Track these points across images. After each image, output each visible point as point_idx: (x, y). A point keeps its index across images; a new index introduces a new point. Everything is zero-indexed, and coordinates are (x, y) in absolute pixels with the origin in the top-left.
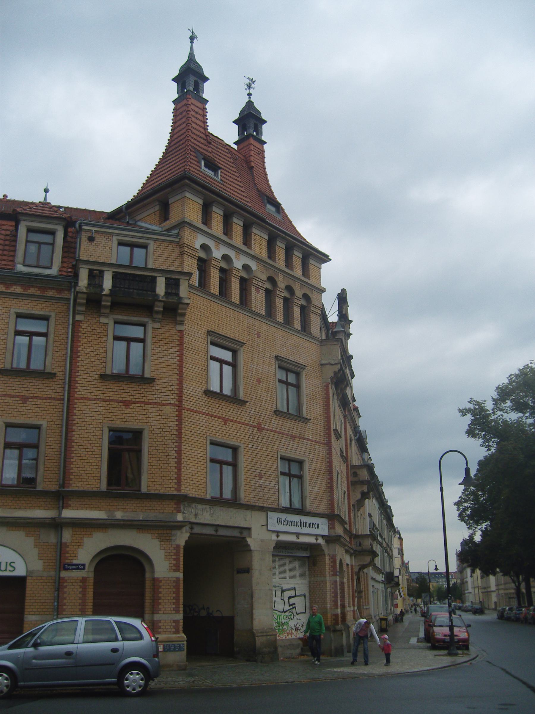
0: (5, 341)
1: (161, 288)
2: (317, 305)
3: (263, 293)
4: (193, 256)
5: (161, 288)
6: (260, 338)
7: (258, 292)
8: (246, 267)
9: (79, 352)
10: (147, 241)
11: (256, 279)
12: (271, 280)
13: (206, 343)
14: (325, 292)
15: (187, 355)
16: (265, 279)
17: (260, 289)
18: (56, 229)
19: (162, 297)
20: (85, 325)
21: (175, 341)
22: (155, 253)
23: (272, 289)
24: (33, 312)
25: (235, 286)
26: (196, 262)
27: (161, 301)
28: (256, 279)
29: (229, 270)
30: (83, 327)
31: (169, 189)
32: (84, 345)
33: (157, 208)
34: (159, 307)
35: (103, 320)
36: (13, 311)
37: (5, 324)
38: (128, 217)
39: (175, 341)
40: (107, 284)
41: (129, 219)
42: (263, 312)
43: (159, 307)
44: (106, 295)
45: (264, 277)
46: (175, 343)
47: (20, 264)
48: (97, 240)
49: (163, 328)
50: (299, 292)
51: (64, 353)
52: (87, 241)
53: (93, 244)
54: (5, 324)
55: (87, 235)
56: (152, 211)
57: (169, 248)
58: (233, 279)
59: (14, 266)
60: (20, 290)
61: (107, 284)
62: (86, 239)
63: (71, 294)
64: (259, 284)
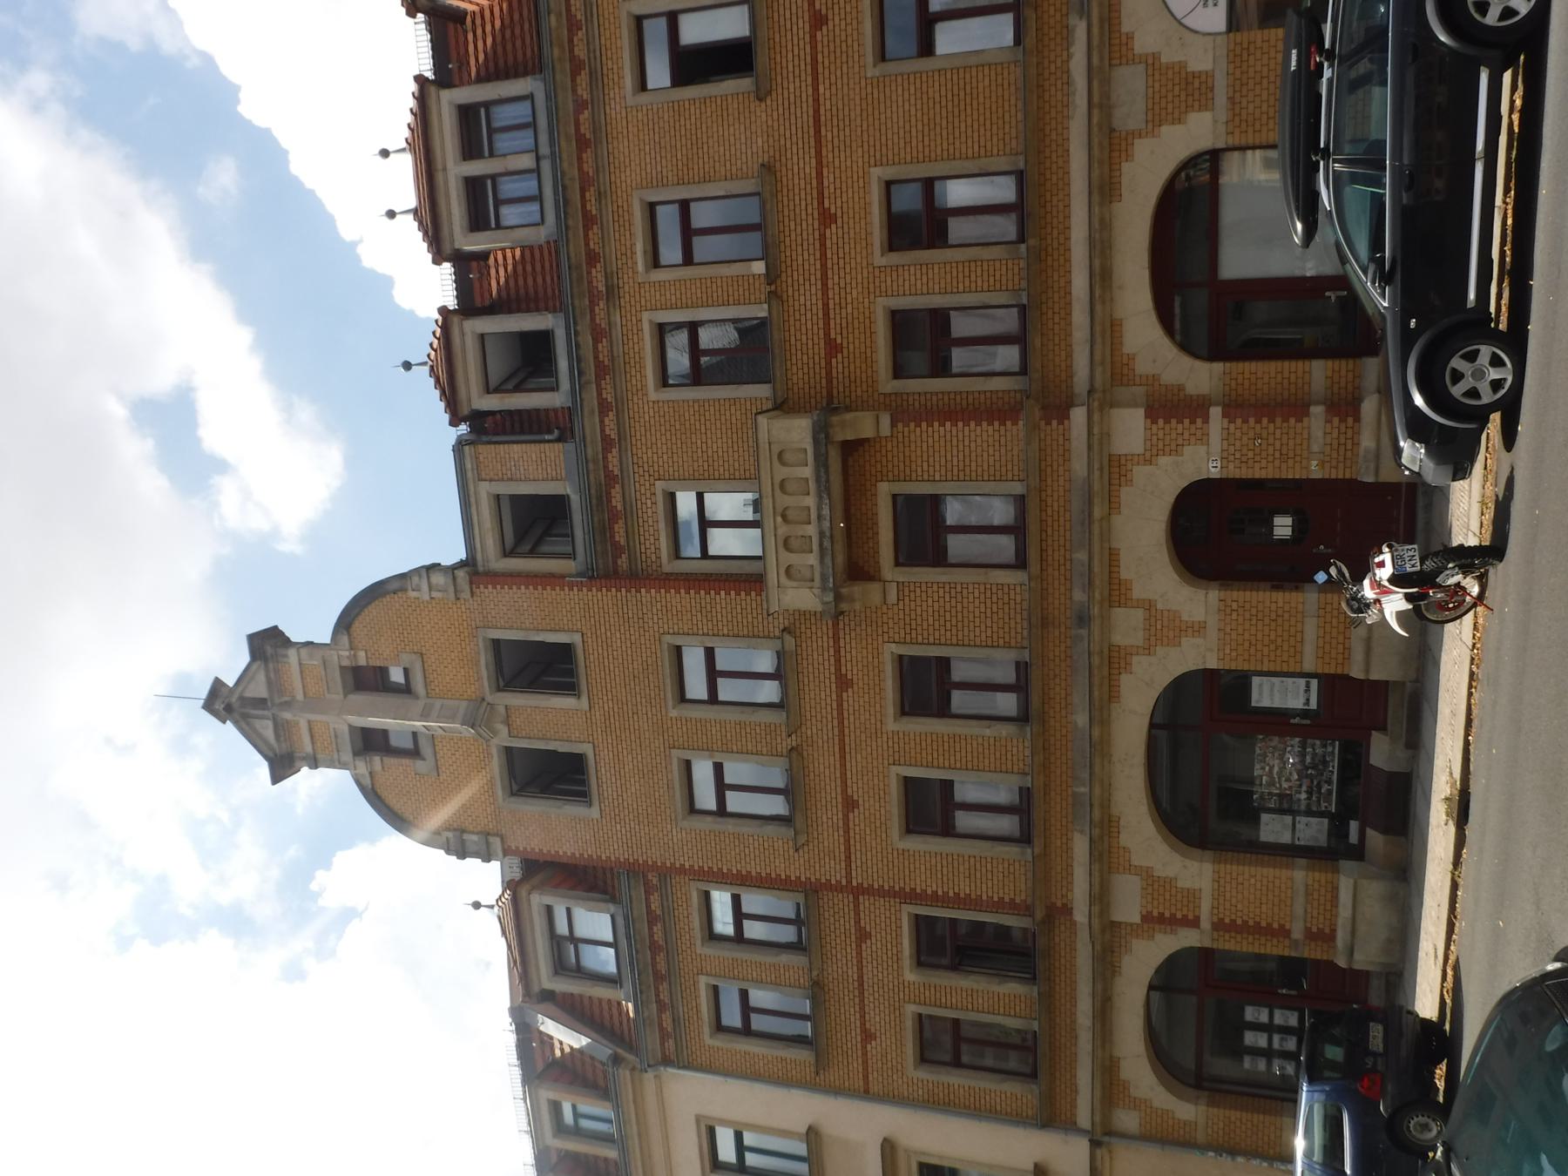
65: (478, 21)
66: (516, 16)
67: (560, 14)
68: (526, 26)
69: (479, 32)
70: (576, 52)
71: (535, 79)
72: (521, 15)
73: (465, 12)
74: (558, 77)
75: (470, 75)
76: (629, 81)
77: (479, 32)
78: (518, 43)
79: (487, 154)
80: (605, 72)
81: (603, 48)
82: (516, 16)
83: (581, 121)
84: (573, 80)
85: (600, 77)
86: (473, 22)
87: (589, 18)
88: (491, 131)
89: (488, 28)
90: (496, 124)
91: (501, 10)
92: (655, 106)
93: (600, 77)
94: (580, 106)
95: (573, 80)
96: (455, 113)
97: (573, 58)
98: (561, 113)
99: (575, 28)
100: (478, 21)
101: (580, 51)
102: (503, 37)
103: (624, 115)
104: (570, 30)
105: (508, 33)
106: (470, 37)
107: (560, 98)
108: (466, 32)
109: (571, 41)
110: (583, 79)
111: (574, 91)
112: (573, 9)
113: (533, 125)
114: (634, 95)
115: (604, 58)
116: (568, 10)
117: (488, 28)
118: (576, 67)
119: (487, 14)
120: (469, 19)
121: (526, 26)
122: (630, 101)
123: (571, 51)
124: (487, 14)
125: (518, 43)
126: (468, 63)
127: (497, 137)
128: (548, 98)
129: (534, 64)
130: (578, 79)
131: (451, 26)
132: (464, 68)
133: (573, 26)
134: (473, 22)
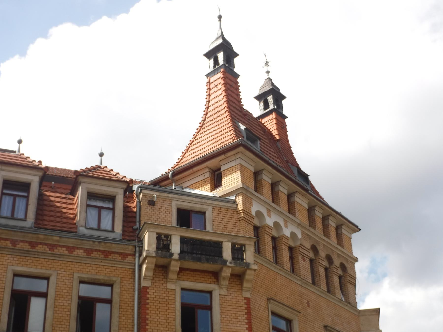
0: (69, 308)
1: (227, 254)
2: (353, 275)
3: (308, 261)
4: (249, 222)
5: (227, 254)
6: (310, 307)
7: (304, 260)
8: (293, 234)
9: (147, 319)
10: (205, 207)
11: (302, 247)
12: (314, 249)
13: (267, 312)
14: (358, 261)
15: (254, 322)
16: (309, 248)
17: (305, 258)
18: (117, 193)
19: (231, 263)
20: (152, 291)
21: (242, 308)
22: (214, 218)
23: (314, 258)
24: (98, 277)
25: (285, 253)
26: (252, 228)
27: (229, 267)
28: (302, 247)
29: (279, 237)
30: (150, 293)
31: (223, 157)
32: (152, 312)
33: (208, 175)
34: (227, 273)
35: (171, 286)
36: (76, 275)
37: (68, 289)
38: (174, 185)
39: (242, 308)
40: (176, 248)
41: (175, 186)
42: (310, 280)
43: (227, 273)
44: (175, 260)
45: (308, 246)
46: (242, 311)
47: (82, 226)
48: (157, 205)
49: (230, 294)
50: (337, 262)
51: (131, 321)
52: (148, 206)
53: (153, 208)
54: (68, 289)
55: (146, 199)
56: (201, 178)
57: (226, 214)
58: (284, 247)
59: (76, 228)
60: (83, 254)
61: (176, 248)
62: (146, 203)
63: (135, 259)
64: (305, 252)
65: (69, 201)
66: (65, 220)
67: (59, 242)
68: (58, 224)
69: (64, 201)
70: (40, 246)
71: (32, 224)
72: (64, 223)
73: (74, 196)
74: (30, 235)
75: (46, 191)
76: (20, 269)
77: (64, 201)
78: (52, 219)
79: (5, 191)
80: (27, 258)
81: (38, 259)
82: (65, 220)
83: (7, 242)
84: (27, 242)
85: (25, 255)
86: (69, 199)
87: (54, 255)
88: (15, 196)
89: (64, 205)
90: (17, 199)
91: (70, 214)
92: (4, 279)
93: (25, 255)
94: (14, 243)
95: (27, 242)
96: (28, 181)
97: (37, 244)
98: (12, 233)
99: (51, 247)
100: (69, 201)
101: (40, 248)
102: (58, 212)
103: (5, 263)
104: (50, 245)
105: (58, 214)
106: (64, 196)
107: (19, 234)
108: (66, 194)
109: (46, 244)
110: (26, 247)
111: (22, 241)
112: (60, 248)
113: (12, 217)
114: (13, 270)
115: (34, 259)
116: (60, 246)
117: (64, 205)
118: (33, 245)
119: (71, 206)
120: (71, 197)
121: (58, 224)
122: (11, 268)
123: (41, 244)
124: (71, 206)
125: (52, 219)
126: (52, 192)
127: (12, 198)
128: (21, 228)
129: (40, 224)
130: (27, 244)
131: (70, 187)
132: (50, 189)
133: (52, 247)
134: (69, 199)
